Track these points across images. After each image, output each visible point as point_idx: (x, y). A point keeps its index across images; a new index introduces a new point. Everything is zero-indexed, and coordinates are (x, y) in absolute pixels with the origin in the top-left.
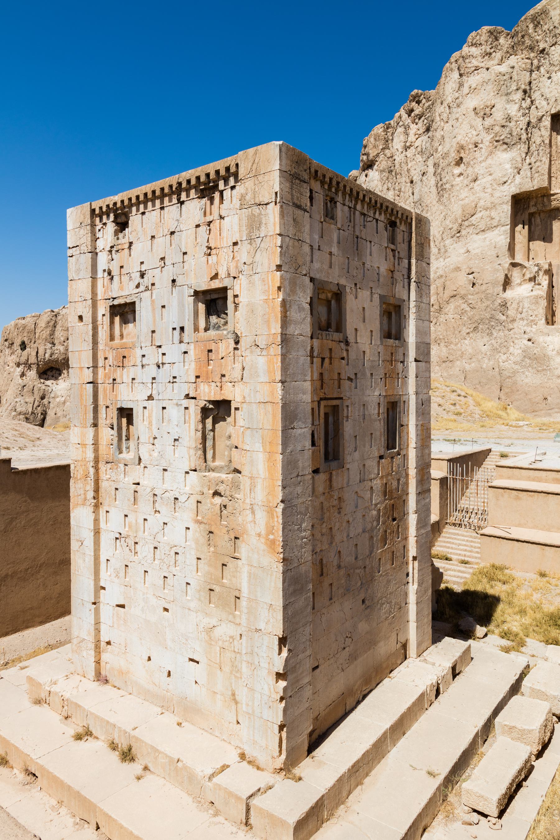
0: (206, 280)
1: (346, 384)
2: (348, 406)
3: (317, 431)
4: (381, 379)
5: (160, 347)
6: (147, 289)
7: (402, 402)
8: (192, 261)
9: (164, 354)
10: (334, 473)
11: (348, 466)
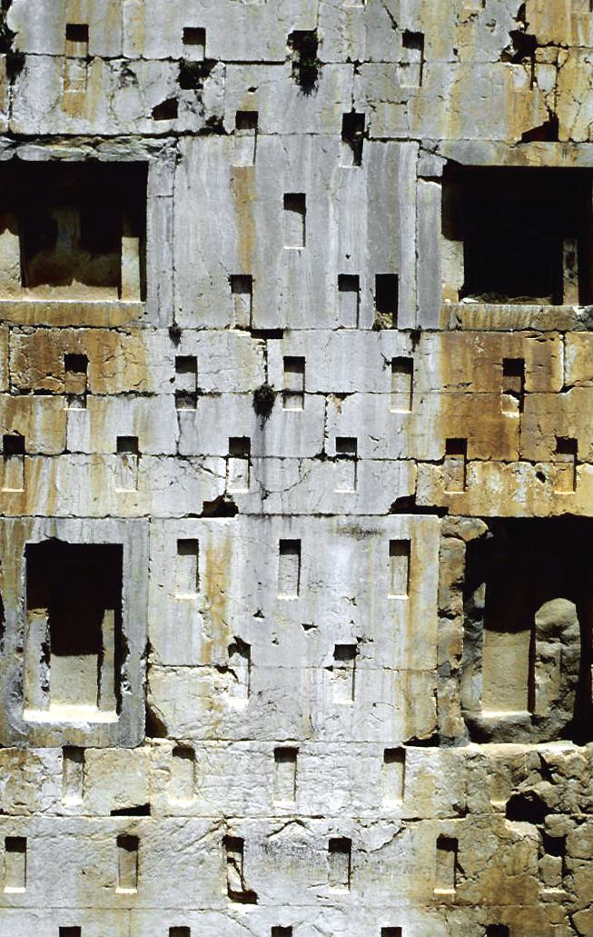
0: (503, 137)
5: (278, 334)
6: (214, 127)
8: (448, 68)
9: (294, 364)
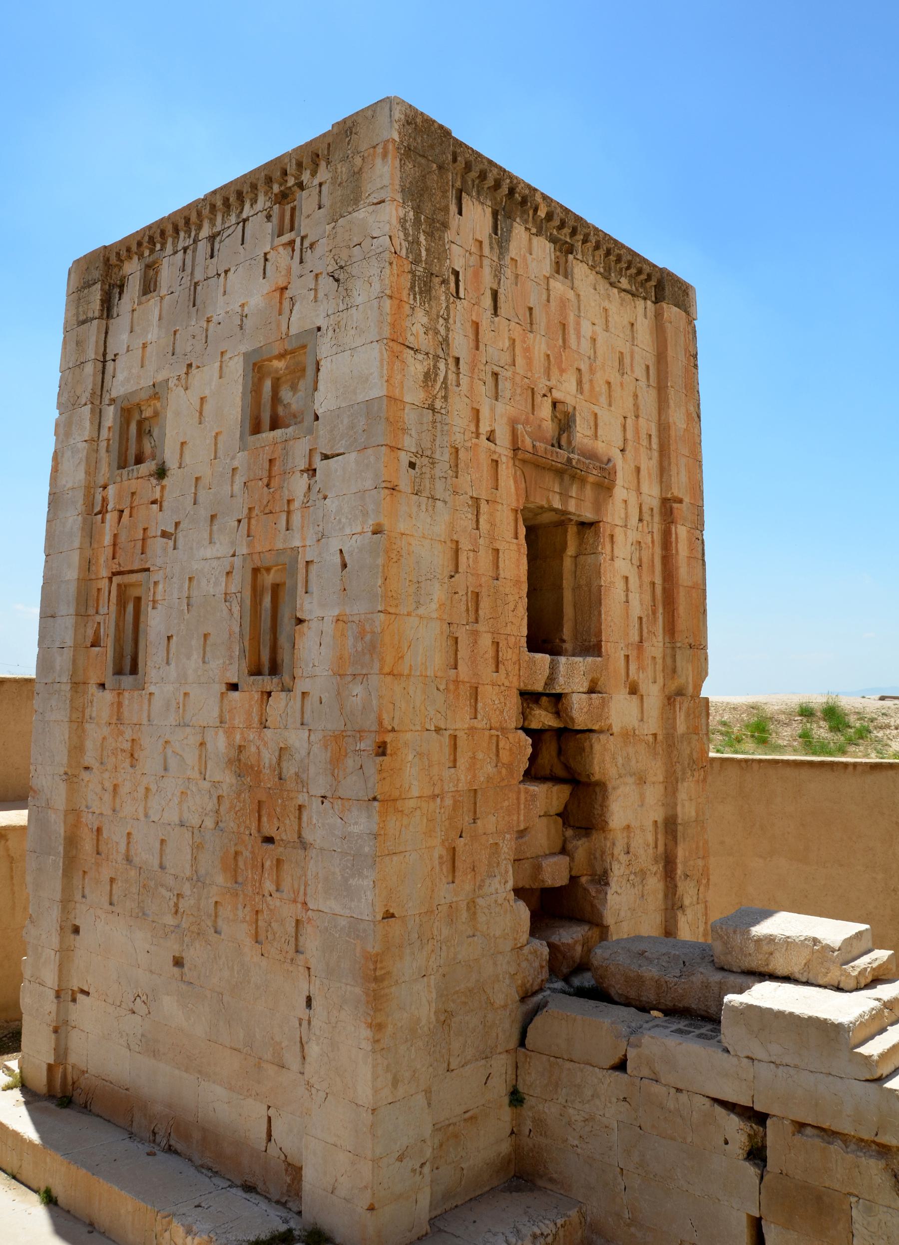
1: (157, 544)
2: (156, 583)
3: (105, 623)
4: (239, 521)
7: (301, 565)
10: (126, 694)
11: (152, 689)
